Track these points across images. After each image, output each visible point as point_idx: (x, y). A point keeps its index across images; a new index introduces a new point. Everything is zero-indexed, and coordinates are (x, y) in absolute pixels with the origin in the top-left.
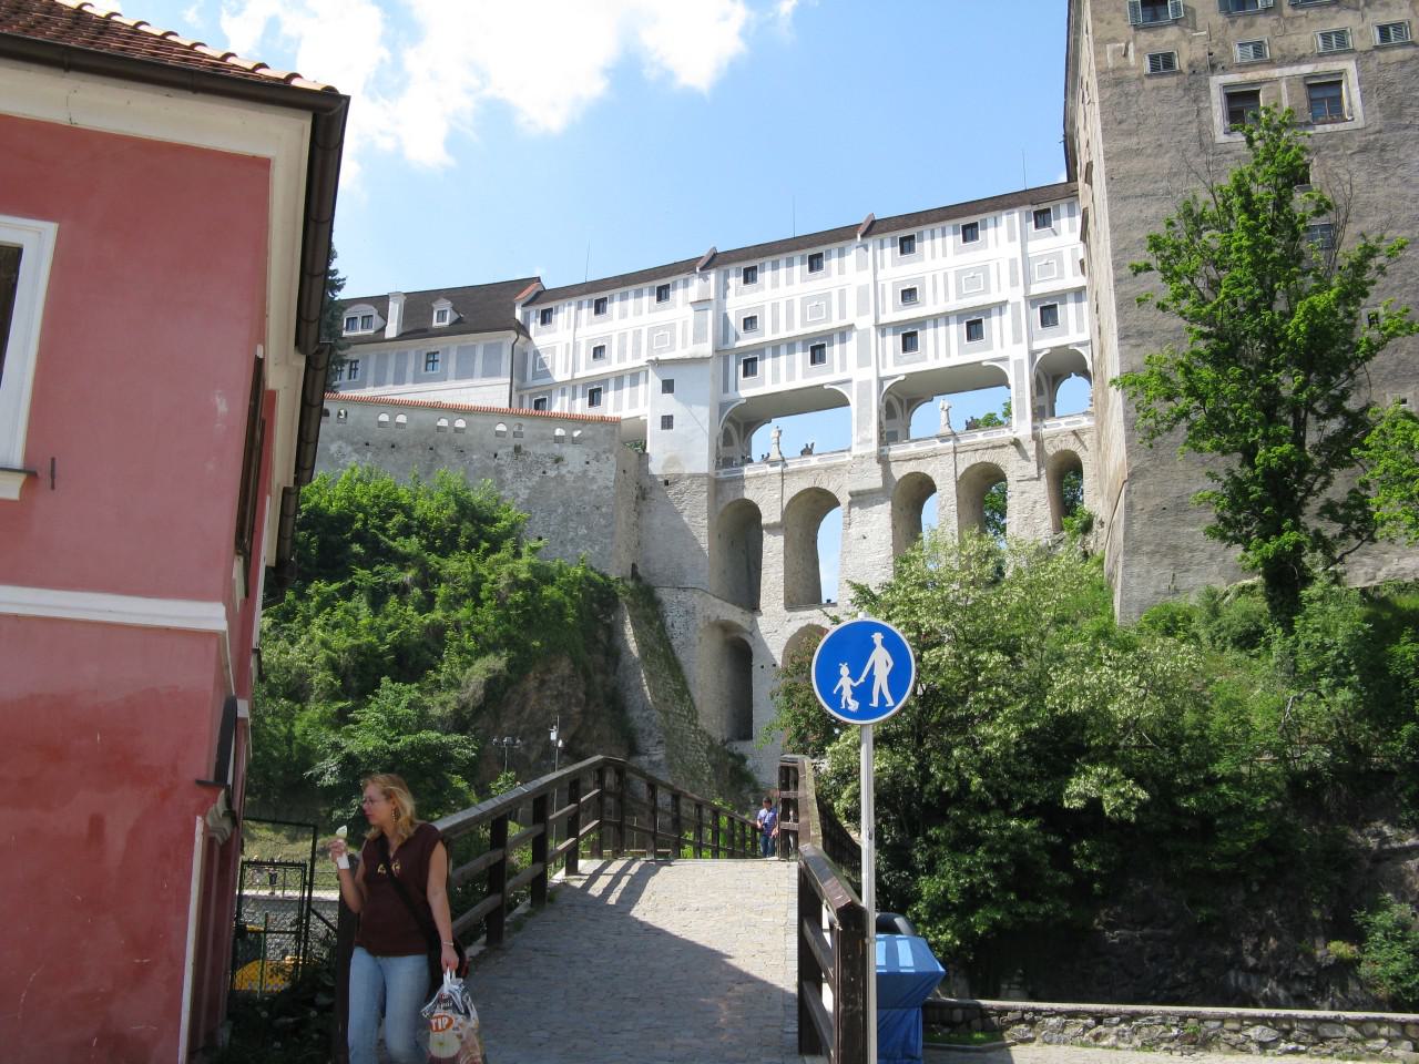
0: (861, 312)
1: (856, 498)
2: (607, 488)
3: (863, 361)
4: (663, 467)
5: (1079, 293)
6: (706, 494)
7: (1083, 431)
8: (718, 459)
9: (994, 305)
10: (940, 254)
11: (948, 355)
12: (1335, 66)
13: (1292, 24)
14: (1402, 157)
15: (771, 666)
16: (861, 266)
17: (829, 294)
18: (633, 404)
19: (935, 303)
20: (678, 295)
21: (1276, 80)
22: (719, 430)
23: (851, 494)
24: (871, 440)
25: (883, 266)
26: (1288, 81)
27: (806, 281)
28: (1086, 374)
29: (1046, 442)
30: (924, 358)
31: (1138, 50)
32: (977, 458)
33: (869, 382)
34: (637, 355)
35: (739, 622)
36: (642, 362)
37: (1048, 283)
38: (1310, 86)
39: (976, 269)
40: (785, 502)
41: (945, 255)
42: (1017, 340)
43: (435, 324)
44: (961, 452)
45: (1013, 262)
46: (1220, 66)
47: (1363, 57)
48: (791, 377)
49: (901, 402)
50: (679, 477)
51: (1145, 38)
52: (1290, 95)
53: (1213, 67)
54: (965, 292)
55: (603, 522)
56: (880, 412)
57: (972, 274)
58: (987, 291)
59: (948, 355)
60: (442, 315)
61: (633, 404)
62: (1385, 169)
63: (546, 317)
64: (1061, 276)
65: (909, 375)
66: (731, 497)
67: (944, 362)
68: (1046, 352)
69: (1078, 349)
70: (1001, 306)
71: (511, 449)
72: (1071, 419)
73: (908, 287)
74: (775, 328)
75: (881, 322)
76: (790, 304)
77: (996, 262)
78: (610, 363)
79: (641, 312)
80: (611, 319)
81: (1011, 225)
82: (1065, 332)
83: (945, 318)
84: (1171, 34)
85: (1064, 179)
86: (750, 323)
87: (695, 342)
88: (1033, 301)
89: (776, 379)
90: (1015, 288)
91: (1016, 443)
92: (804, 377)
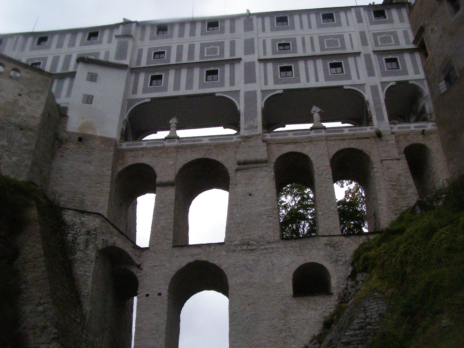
1: (242, 167)
2: (34, 117)
4: (80, 128)
5: (410, 51)
6: (112, 153)
7: (431, 132)
15: (156, 295)
17: (223, 43)
22: (126, 117)
23: (239, 163)
25: (264, 30)
27: (205, 35)
33: (255, 92)
35: (130, 253)
40: (179, 166)
42: (371, 73)
50: (93, 137)
55: (24, 141)
57: (332, 39)
59: (317, 80)
65: (285, 91)
66: (130, 161)
67: (313, 84)
68: (391, 84)
69: (414, 83)
70: (357, 54)
86: (159, 54)
89: (177, 87)
90: (365, 47)
92: (200, 88)
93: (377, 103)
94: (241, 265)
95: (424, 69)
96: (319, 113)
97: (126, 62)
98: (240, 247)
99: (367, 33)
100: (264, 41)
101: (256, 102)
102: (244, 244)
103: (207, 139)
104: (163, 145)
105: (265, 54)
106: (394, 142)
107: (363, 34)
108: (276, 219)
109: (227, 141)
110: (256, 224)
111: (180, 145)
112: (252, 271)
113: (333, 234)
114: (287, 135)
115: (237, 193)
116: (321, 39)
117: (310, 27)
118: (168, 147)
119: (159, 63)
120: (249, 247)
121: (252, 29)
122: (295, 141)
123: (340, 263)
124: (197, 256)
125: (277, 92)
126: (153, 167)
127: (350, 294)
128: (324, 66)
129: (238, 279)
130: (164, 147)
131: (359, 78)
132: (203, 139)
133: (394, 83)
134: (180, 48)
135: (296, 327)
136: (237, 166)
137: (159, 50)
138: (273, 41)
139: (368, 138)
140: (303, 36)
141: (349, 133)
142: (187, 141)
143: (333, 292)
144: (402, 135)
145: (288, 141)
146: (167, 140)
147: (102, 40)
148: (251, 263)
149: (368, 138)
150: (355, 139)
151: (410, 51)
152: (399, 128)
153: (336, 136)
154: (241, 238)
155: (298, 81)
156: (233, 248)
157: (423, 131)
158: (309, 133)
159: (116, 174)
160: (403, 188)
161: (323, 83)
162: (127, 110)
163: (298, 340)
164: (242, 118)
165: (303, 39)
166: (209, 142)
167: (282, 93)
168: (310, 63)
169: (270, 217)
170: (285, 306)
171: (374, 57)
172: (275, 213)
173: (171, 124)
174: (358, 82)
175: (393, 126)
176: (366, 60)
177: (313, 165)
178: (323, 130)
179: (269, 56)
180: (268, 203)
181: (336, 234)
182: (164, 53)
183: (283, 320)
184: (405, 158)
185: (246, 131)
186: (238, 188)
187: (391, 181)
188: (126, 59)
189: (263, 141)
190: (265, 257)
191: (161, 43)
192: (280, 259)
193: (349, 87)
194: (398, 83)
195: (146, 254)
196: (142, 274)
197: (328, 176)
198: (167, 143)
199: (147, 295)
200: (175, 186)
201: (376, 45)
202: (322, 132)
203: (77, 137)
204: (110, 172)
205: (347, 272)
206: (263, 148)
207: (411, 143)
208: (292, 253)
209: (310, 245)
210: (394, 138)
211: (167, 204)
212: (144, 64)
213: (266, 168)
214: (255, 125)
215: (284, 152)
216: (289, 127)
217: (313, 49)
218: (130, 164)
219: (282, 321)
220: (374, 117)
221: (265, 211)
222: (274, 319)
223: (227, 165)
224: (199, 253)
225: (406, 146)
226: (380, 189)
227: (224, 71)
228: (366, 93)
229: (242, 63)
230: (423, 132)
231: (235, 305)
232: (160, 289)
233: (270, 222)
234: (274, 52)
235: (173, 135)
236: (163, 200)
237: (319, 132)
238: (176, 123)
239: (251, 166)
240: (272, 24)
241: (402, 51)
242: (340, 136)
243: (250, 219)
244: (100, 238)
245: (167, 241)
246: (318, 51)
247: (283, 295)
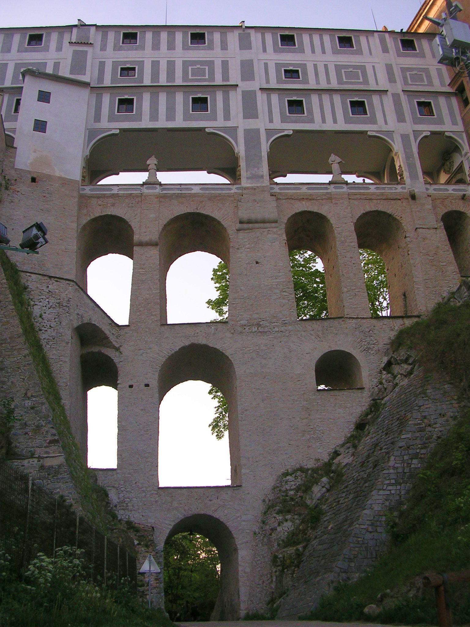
1: (245, 226)
15: (143, 386)
24: (262, 176)
25: (265, 50)
33: (258, 131)
35: (107, 332)
42: (401, 118)
48: (171, 116)
54: (345, 80)
59: (335, 121)
67: (329, 126)
68: (424, 134)
77: (372, 64)
79: (9, 51)
86: (127, 71)
89: (154, 116)
93: (408, 156)
94: (251, 351)
95: (463, 119)
96: (339, 163)
97: (85, 78)
98: (248, 328)
99: (394, 66)
100: (266, 65)
101: (260, 143)
102: (253, 325)
103: (198, 188)
104: (139, 192)
105: (268, 82)
106: (430, 207)
107: (389, 69)
108: (291, 294)
109: (224, 192)
110: (266, 300)
111: (162, 194)
112: (265, 359)
113: (362, 317)
114: (299, 189)
115: (240, 260)
116: (338, 68)
117: (324, 52)
118: (147, 196)
119: (127, 82)
120: (259, 328)
121: (250, 48)
122: (310, 198)
123: (372, 352)
124: (193, 338)
126: (128, 221)
127: (386, 389)
128: (343, 103)
129: (247, 368)
132: (192, 187)
133: (429, 134)
134: (155, 65)
135: (321, 428)
136: (239, 226)
137: (128, 66)
138: (278, 66)
139: (399, 199)
140: (315, 63)
141: (375, 191)
142: (172, 189)
143: (365, 386)
144: (439, 199)
145: (302, 197)
146: (145, 186)
147: (49, 46)
148: (265, 348)
149: (399, 199)
150: (383, 199)
151: (446, 94)
152: (435, 190)
153: (361, 194)
154: (248, 316)
155: (312, 121)
156: (240, 329)
157: (464, 195)
158: (327, 189)
160: (442, 264)
161: (342, 126)
163: (325, 444)
164: (242, 164)
165: (315, 66)
166: (201, 192)
167: (291, 135)
168: (326, 98)
169: (284, 292)
170: (307, 402)
172: (290, 287)
173: (149, 165)
174: (384, 128)
176: (394, 100)
177: (334, 228)
178: (344, 186)
179: (273, 84)
180: (280, 274)
181: (365, 317)
182: (134, 69)
183: (306, 420)
184: (443, 227)
185: (249, 181)
186: (241, 253)
187: (428, 255)
188: (85, 74)
189: (272, 195)
190: (280, 342)
192: (299, 345)
193: (374, 134)
194: (433, 133)
195: (126, 333)
196: (122, 359)
197: (352, 244)
198: (145, 190)
199: (131, 386)
200: (159, 247)
201: (406, 83)
202: (343, 188)
203: (30, 177)
205: (380, 362)
206: (272, 204)
207: (450, 209)
208: (313, 337)
209: (335, 328)
210: (431, 202)
211: (150, 270)
213: (275, 230)
214: (261, 173)
215: (297, 211)
216: (292, 178)
217: (328, 81)
219: (304, 421)
220: (406, 175)
221: (278, 284)
222: (294, 418)
223: (225, 223)
224: (196, 334)
225: (444, 212)
226: (415, 263)
227: (215, 100)
228: (396, 143)
229: (239, 90)
230: (463, 197)
231: (246, 401)
232: (147, 379)
233: (284, 299)
234: (279, 81)
235: (152, 180)
236: (144, 265)
237: (339, 188)
238: (155, 164)
239: (257, 225)
240: (275, 43)
242: (365, 195)
243: (259, 293)
245: (152, 317)
246: (334, 84)
247: (304, 389)
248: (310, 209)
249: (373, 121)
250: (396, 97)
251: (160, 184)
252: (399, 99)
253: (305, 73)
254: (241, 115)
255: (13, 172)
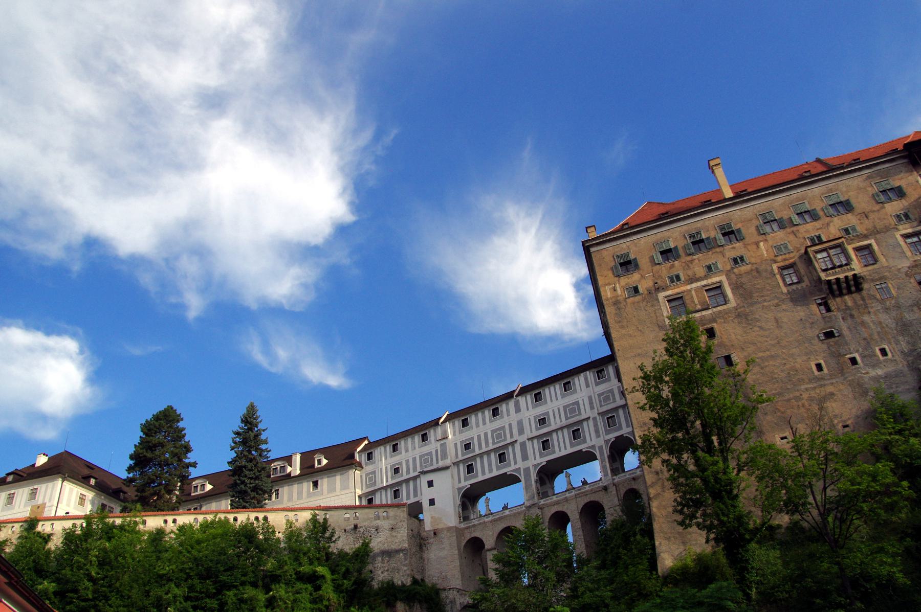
0: (521, 431)
2: (403, 540)
3: (525, 457)
6: (455, 537)
8: (460, 517)
9: (584, 420)
10: (554, 399)
11: (566, 449)
12: (715, 279)
13: (692, 263)
14: (757, 317)
16: (518, 410)
17: (504, 427)
18: (415, 495)
19: (556, 424)
20: (431, 434)
21: (690, 290)
22: (458, 502)
25: (528, 409)
26: (695, 290)
28: (635, 448)
29: (620, 486)
30: (554, 452)
31: (623, 288)
32: (586, 500)
33: (529, 468)
34: (415, 469)
36: (416, 474)
37: (608, 405)
38: (706, 290)
39: (573, 404)
40: (496, 535)
41: (557, 399)
42: (598, 436)
43: (316, 466)
44: (580, 497)
45: (590, 398)
46: (661, 289)
47: (728, 274)
48: (491, 471)
49: (547, 474)
51: (624, 281)
52: (697, 296)
53: (658, 289)
56: (536, 482)
57: (571, 407)
58: (580, 414)
59: (566, 449)
60: (320, 462)
61: (415, 495)
62: (750, 324)
63: (370, 457)
64: (615, 401)
66: (468, 537)
67: (564, 452)
71: (353, 526)
72: (631, 472)
73: (542, 417)
74: (480, 447)
75: (530, 437)
76: (486, 434)
78: (402, 476)
79: (415, 449)
80: (401, 453)
81: (586, 379)
82: (620, 428)
83: (562, 428)
84: (636, 276)
85: (610, 353)
87: (442, 460)
88: (602, 414)
89: (483, 473)
91: (605, 488)
100: (529, 419)
101: (530, 476)
125: (543, 464)
128: (569, 434)
130: (485, 522)
131: (591, 440)
138: (535, 418)
153: (582, 493)
159: (462, 548)
162: (459, 495)
171: (599, 419)
175: (614, 477)
178: (573, 491)
191: (467, 434)
202: (572, 492)
204: (457, 551)
212: (460, 458)
218: (468, 538)
229: (518, 442)
241: (616, 409)
244: (458, 603)
248: (559, 510)
249: (585, 441)
250: (594, 419)
251: (492, 514)
252: (597, 421)
253: (549, 419)
254: (521, 459)
255: (425, 533)
